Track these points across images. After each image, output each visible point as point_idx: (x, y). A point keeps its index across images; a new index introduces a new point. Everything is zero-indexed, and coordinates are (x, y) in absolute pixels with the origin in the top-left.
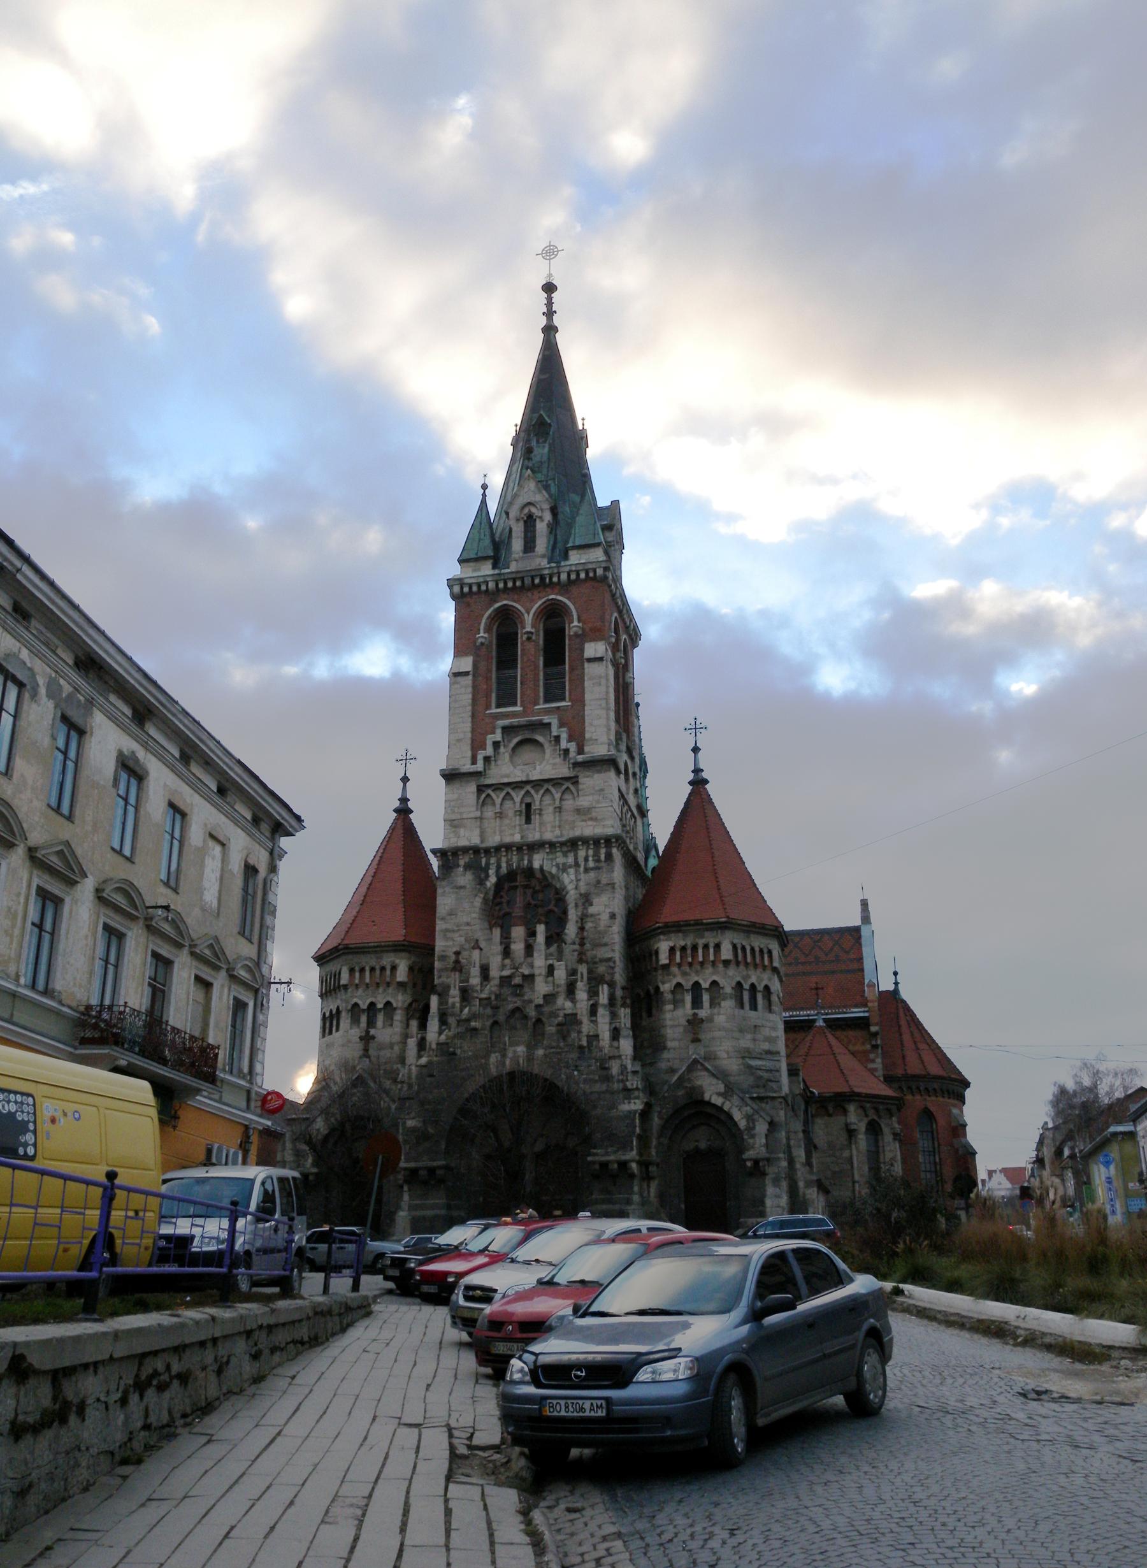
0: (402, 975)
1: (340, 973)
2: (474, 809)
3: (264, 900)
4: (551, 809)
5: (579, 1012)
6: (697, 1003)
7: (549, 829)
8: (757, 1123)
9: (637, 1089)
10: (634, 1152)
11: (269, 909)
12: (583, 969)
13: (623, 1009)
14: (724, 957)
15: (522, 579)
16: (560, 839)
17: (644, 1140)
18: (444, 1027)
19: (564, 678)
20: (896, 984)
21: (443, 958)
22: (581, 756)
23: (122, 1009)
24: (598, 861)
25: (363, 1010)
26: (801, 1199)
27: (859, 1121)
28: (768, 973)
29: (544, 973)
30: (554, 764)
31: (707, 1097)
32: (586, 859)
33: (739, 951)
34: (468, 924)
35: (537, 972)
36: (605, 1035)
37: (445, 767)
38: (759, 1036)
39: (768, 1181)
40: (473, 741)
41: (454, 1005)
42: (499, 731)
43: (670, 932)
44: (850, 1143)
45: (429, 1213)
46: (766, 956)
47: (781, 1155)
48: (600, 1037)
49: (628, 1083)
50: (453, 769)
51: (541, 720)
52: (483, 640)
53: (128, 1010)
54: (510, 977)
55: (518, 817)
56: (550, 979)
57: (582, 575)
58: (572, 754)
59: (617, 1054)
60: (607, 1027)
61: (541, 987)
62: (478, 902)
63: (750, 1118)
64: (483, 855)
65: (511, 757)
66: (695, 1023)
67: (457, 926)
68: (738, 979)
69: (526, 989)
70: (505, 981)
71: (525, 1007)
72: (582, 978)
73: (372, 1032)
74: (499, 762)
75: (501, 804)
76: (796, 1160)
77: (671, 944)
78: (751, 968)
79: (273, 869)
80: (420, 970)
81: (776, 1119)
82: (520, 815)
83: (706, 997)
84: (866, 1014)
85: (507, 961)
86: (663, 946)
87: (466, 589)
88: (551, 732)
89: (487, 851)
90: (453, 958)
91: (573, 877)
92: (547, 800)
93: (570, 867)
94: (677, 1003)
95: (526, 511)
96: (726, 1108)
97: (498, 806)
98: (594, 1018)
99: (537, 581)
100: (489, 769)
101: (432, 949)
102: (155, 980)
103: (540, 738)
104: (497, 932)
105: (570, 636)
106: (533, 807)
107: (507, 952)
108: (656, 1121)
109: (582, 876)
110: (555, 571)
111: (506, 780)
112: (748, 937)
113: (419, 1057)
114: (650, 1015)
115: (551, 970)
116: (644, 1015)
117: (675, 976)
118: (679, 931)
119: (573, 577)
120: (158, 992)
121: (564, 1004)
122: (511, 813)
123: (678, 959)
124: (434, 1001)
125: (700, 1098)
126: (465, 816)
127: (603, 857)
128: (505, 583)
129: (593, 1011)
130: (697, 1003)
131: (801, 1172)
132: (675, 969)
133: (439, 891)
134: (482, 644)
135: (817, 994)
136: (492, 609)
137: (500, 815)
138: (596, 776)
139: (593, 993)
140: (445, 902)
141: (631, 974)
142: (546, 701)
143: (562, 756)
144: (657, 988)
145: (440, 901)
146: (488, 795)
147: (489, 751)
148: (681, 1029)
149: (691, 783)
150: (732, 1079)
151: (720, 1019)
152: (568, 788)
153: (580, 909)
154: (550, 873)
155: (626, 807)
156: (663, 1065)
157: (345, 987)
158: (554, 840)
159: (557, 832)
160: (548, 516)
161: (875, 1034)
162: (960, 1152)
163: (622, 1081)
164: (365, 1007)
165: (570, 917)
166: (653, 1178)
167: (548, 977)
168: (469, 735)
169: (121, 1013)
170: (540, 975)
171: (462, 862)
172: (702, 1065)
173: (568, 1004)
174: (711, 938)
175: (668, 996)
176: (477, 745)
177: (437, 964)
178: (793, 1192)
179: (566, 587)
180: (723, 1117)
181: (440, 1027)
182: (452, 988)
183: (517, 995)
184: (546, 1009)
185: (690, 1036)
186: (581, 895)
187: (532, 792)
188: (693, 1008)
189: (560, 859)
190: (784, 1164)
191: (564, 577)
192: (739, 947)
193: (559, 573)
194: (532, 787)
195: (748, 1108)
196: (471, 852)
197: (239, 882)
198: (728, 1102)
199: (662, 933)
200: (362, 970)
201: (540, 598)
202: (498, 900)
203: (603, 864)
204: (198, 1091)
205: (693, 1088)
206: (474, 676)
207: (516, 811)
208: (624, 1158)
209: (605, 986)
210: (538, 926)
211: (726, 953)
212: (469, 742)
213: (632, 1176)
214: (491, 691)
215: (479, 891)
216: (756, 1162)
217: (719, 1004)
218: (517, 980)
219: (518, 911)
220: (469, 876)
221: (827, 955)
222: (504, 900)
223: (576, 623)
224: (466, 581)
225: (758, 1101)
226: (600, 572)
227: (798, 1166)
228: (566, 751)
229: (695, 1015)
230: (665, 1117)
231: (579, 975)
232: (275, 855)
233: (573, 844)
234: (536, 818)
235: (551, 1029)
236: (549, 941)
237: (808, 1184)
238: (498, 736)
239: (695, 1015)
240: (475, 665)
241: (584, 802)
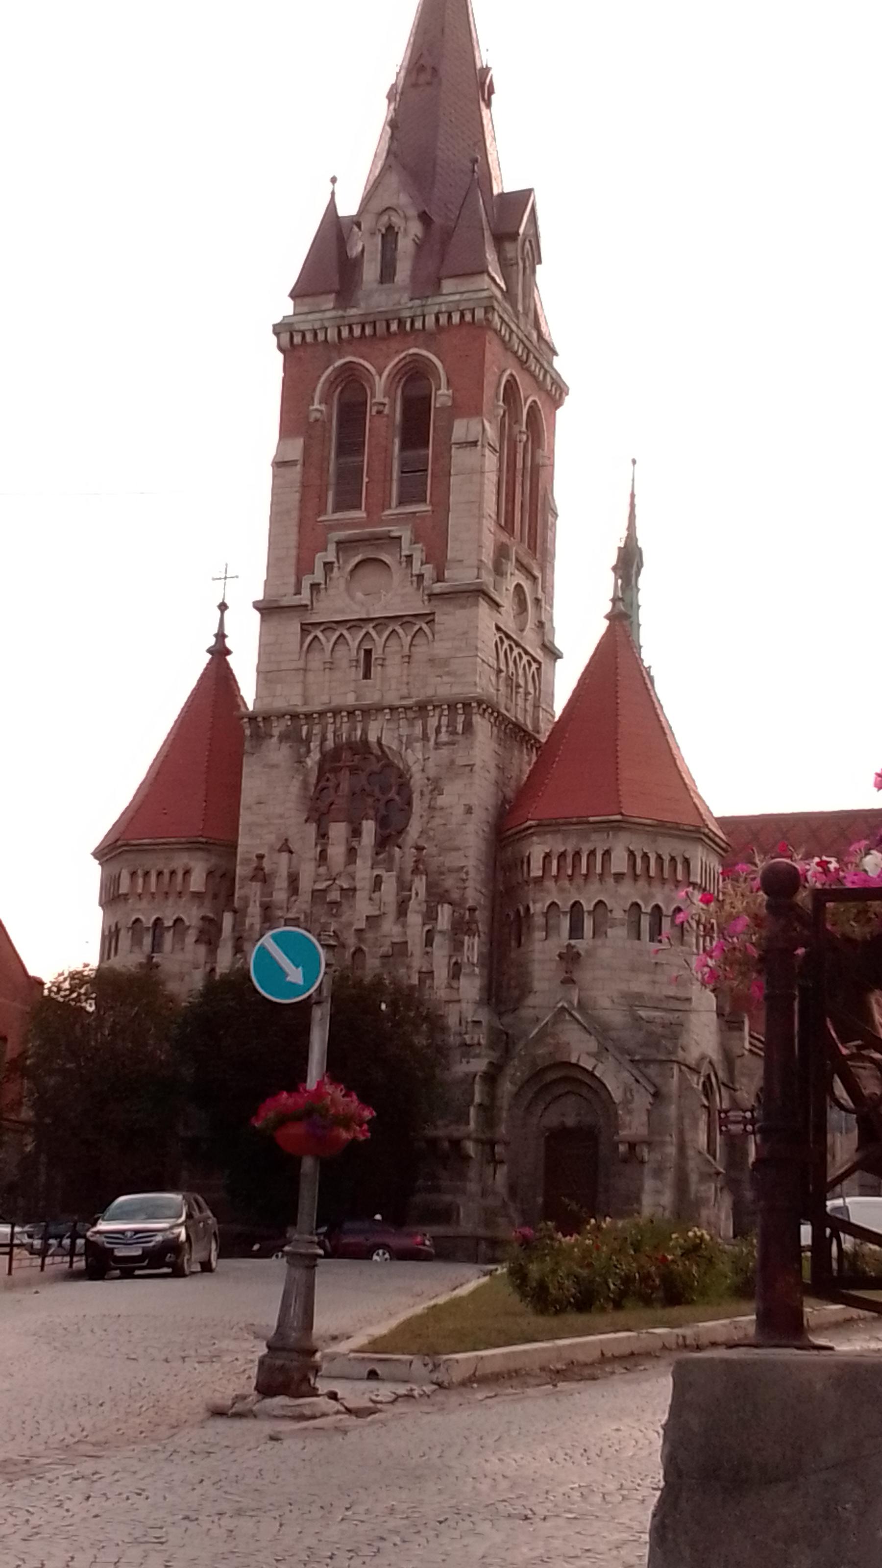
0: (197, 882)
2: (296, 657)
4: (397, 658)
5: (409, 944)
6: (576, 931)
7: (393, 687)
8: (634, 1093)
9: (479, 1044)
10: (472, 1125)
12: (420, 885)
13: (466, 938)
14: (613, 871)
15: (375, 323)
16: (404, 702)
17: (488, 1111)
18: (239, 956)
19: (426, 470)
21: (246, 861)
22: (440, 584)
24: (454, 733)
25: (148, 929)
26: (692, 1196)
31: (574, 1060)
32: (438, 731)
33: (639, 861)
34: (281, 816)
36: (442, 974)
37: (260, 596)
39: (647, 1169)
40: (299, 560)
41: (252, 925)
42: (332, 547)
43: (546, 833)
46: (680, 867)
47: (668, 1138)
48: (435, 974)
49: (466, 1037)
50: (271, 601)
51: (390, 531)
52: (318, 415)
54: (324, 891)
55: (354, 669)
56: (376, 895)
57: (456, 318)
58: (427, 582)
59: (456, 997)
60: (446, 960)
61: (363, 907)
62: (295, 787)
63: (628, 1090)
64: (303, 722)
65: (348, 583)
67: (267, 819)
68: (634, 900)
69: (345, 907)
70: (318, 895)
71: (342, 932)
72: (417, 894)
74: (331, 592)
75: (333, 650)
76: (690, 1144)
77: (547, 851)
80: (223, 876)
81: (664, 1090)
82: (356, 667)
83: (588, 924)
85: (322, 870)
86: (537, 850)
87: (297, 339)
88: (401, 551)
89: (308, 716)
91: (420, 756)
92: (393, 643)
93: (417, 741)
94: (549, 929)
95: (385, 219)
96: (597, 1073)
98: (428, 949)
99: (394, 327)
100: (318, 601)
101: (234, 846)
104: (312, 828)
105: (435, 408)
106: (374, 657)
107: (323, 857)
108: (507, 1087)
109: (432, 754)
110: (419, 312)
112: (654, 841)
114: (519, 944)
115: (378, 882)
116: (513, 943)
117: (549, 892)
118: (559, 831)
119: (443, 319)
121: (390, 928)
122: (344, 663)
124: (228, 920)
126: (283, 667)
127: (460, 728)
128: (351, 330)
129: (429, 941)
130: (576, 931)
132: (550, 884)
133: (245, 770)
134: (317, 420)
136: (331, 368)
137: (331, 665)
138: (460, 613)
139: (430, 916)
141: (501, 888)
142: (401, 503)
143: (415, 584)
144: (528, 909)
145: (246, 783)
146: (316, 637)
147: (318, 576)
148: (553, 966)
150: (613, 1034)
151: (605, 953)
152: (421, 629)
153: (427, 797)
154: (389, 748)
155: (516, 651)
156: (526, 1013)
157: (126, 895)
158: (397, 703)
159: (404, 691)
160: (415, 228)
163: (460, 1034)
164: (150, 925)
165: (414, 810)
166: (502, 1162)
167: (374, 891)
168: (293, 552)
170: (363, 889)
171: (276, 732)
172: (571, 1015)
173: (396, 929)
174: (599, 843)
175: (539, 920)
176: (303, 566)
177: (240, 871)
178: (682, 1184)
179: (429, 338)
180: (594, 1084)
181: (235, 954)
182: (252, 903)
183: (334, 916)
184: (369, 935)
185: (563, 975)
186: (428, 779)
187: (374, 634)
188: (570, 938)
189: (404, 731)
190: (672, 1150)
191: (430, 321)
193: (424, 316)
194: (374, 627)
195: (626, 1074)
196: (288, 717)
198: (600, 1065)
199: (532, 834)
200: (147, 874)
201: (397, 352)
202: (323, 784)
203: (458, 738)
205: (557, 1046)
206: (304, 465)
207: (351, 661)
208: (456, 1135)
209: (446, 906)
210: (364, 822)
211: (619, 863)
212: (293, 561)
213: (468, 1158)
214: (327, 490)
215: (298, 770)
216: (632, 1146)
217: (606, 933)
218: (334, 895)
222: (331, 784)
223: (443, 391)
224: (297, 327)
225: (641, 1066)
226: (480, 314)
227: (691, 1153)
228: (420, 577)
229: (569, 946)
230: (519, 1083)
231: (414, 892)
233: (422, 708)
234: (375, 670)
235: (372, 963)
237: (705, 1177)
238: (331, 556)
239: (569, 946)
240: (306, 449)
241: (441, 648)
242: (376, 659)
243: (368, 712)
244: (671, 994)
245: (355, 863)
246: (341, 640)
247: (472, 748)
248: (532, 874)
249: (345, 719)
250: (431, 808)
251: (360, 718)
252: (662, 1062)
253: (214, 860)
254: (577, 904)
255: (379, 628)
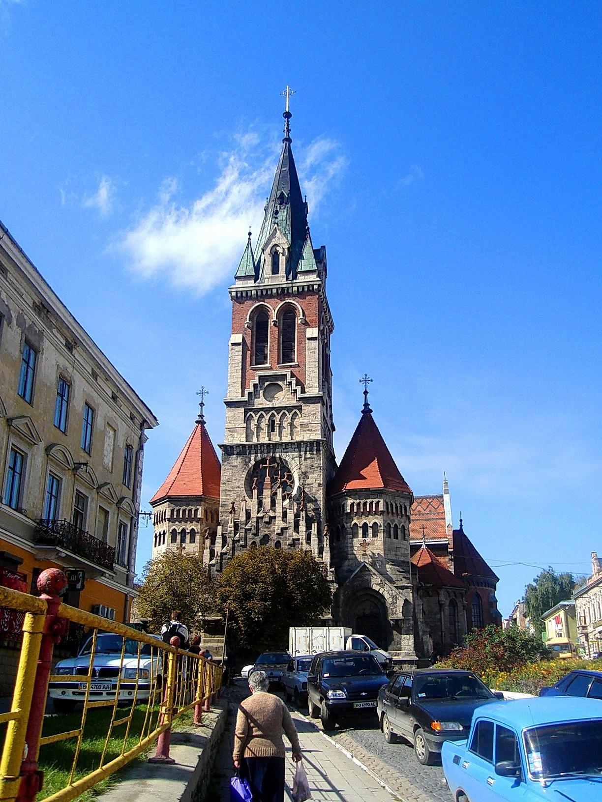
1: (165, 512)
3: (136, 465)
7: (284, 435)
11: (138, 472)
12: (303, 514)
20: (461, 526)
21: (223, 506)
23: (63, 522)
25: (179, 533)
27: (446, 599)
28: (404, 517)
29: (281, 516)
30: (288, 398)
33: (389, 506)
35: (277, 515)
36: (316, 552)
38: (398, 553)
41: (230, 533)
44: (441, 611)
45: (215, 645)
53: (66, 523)
54: (262, 518)
56: (285, 519)
61: (279, 524)
62: (244, 475)
66: (364, 544)
72: (303, 519)
73: (184, 545)
77: (352, 502)
78: (395, 515)
79: (141, 448)
82: (268, 427)
83: (370, 531)
84: (447, 542)
89: (250, 446)
90: (231, 505)
91: (298, 463)
93: (296, 457)
94: (355, 535)
96: (381, 592)
97: (256, 421)
102: (77, 507)
103: (280, 383)
104: (255, 492)
106: (276, 423)
107: (260, 504)
109: (303, 461)
111: (260, 407)
113: (211, 560)
114: (338, 540)
115: (285, 515)
118: (357, 494)
120: (79, 515)
121: (291, 533)
123: (355, 510)
125: (367, 586)
129: (308, 538)
131: (421, 627)
135: (423, 531)
139: (309, 528)
140: (225, 474)
147: (251, 390)
149: (362, 412)
153: (302, 480)
154: (285, 460)
157: (169, 520)
161: (451, 553)
162: (494, 616)
164: (180, 531)
169: (62, 525)
171: (235, 452)
173: (294, 534)
175: (349, 530)
176: (243, 387)
177: (221, 509)
182: (230, 522)
186: (302, 472)
187: (276, 414)
188: (363, 537)
190: (412, 622)
192: (389, 503)
197: (123, 453)
198: (382, 588)
203: (315, 456)
204: (103, 574)
216: (397, 621)
218: (267, 519)
219: (268, 479)
220: (239, 460)
221: (425, 510)
227: (419, 623)
231: (301, 517)
232: (142, 440)
234: (277, 429)
236: (284, 499)
237: (424, 633)
238: (257, 382)
242: (278, 424)
243: (276, 445)
244: (402, 560)
245: (275, 506)
246: (261, 416)
247: (320, 460)
248: (345, 512)
249: (265, 448)
250: (304, 485)
251: (272, 448)
252: (407, 587)
253: (207, 505)
254: (365, 524)
255: (277, 411)
